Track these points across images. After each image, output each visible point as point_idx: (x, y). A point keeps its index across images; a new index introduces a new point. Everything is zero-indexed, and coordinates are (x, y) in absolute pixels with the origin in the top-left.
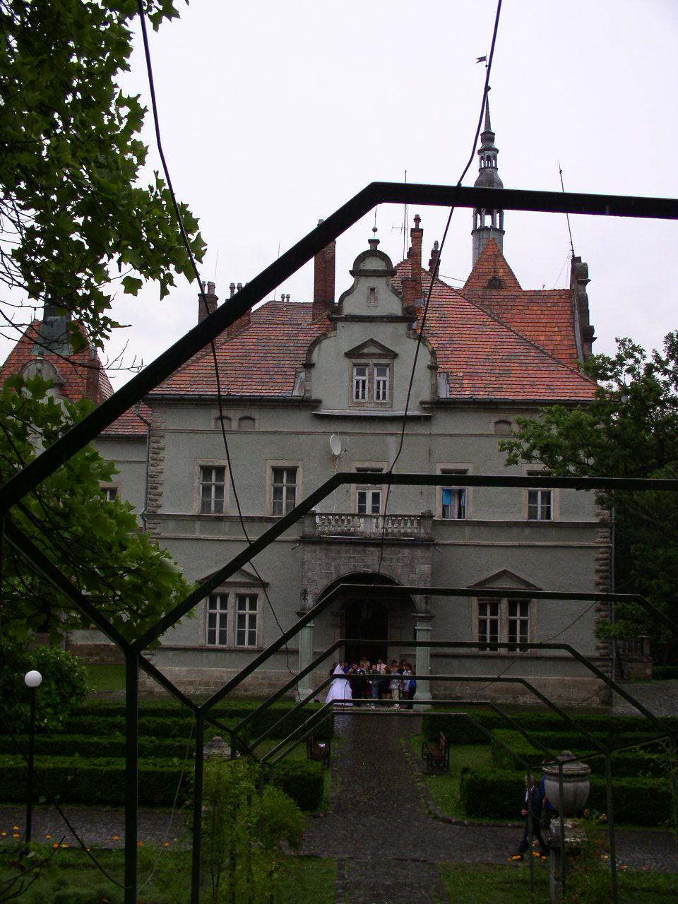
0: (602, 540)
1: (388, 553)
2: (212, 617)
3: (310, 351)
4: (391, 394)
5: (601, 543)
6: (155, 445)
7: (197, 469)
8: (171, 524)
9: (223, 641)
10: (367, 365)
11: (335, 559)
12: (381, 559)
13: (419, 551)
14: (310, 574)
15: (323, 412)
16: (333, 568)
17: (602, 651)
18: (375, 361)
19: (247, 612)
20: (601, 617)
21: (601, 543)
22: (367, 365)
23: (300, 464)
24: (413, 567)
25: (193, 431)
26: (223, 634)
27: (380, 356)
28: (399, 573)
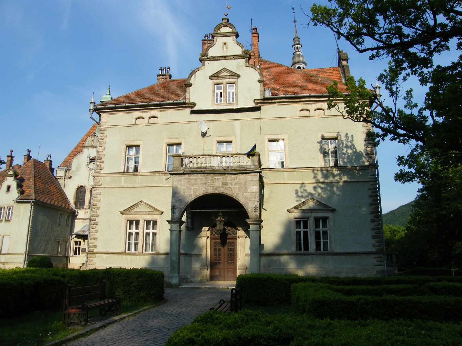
0: (371, 177)
1: (229, 178)
4: (237, 98)
5: (371, 178)
8: (108, 179)
9: (136, 249)
11: (194, 185)
12: (225, 184)
13: (250, 177)
15: (196, 108)
16: (192, 191)
17: (377, 248)
20: (375, 226)
21: (371, 178)
24: (246, 188)
25: (123, 126)
26: (136, 244)
27: (230, 77)
28: (237, 192)
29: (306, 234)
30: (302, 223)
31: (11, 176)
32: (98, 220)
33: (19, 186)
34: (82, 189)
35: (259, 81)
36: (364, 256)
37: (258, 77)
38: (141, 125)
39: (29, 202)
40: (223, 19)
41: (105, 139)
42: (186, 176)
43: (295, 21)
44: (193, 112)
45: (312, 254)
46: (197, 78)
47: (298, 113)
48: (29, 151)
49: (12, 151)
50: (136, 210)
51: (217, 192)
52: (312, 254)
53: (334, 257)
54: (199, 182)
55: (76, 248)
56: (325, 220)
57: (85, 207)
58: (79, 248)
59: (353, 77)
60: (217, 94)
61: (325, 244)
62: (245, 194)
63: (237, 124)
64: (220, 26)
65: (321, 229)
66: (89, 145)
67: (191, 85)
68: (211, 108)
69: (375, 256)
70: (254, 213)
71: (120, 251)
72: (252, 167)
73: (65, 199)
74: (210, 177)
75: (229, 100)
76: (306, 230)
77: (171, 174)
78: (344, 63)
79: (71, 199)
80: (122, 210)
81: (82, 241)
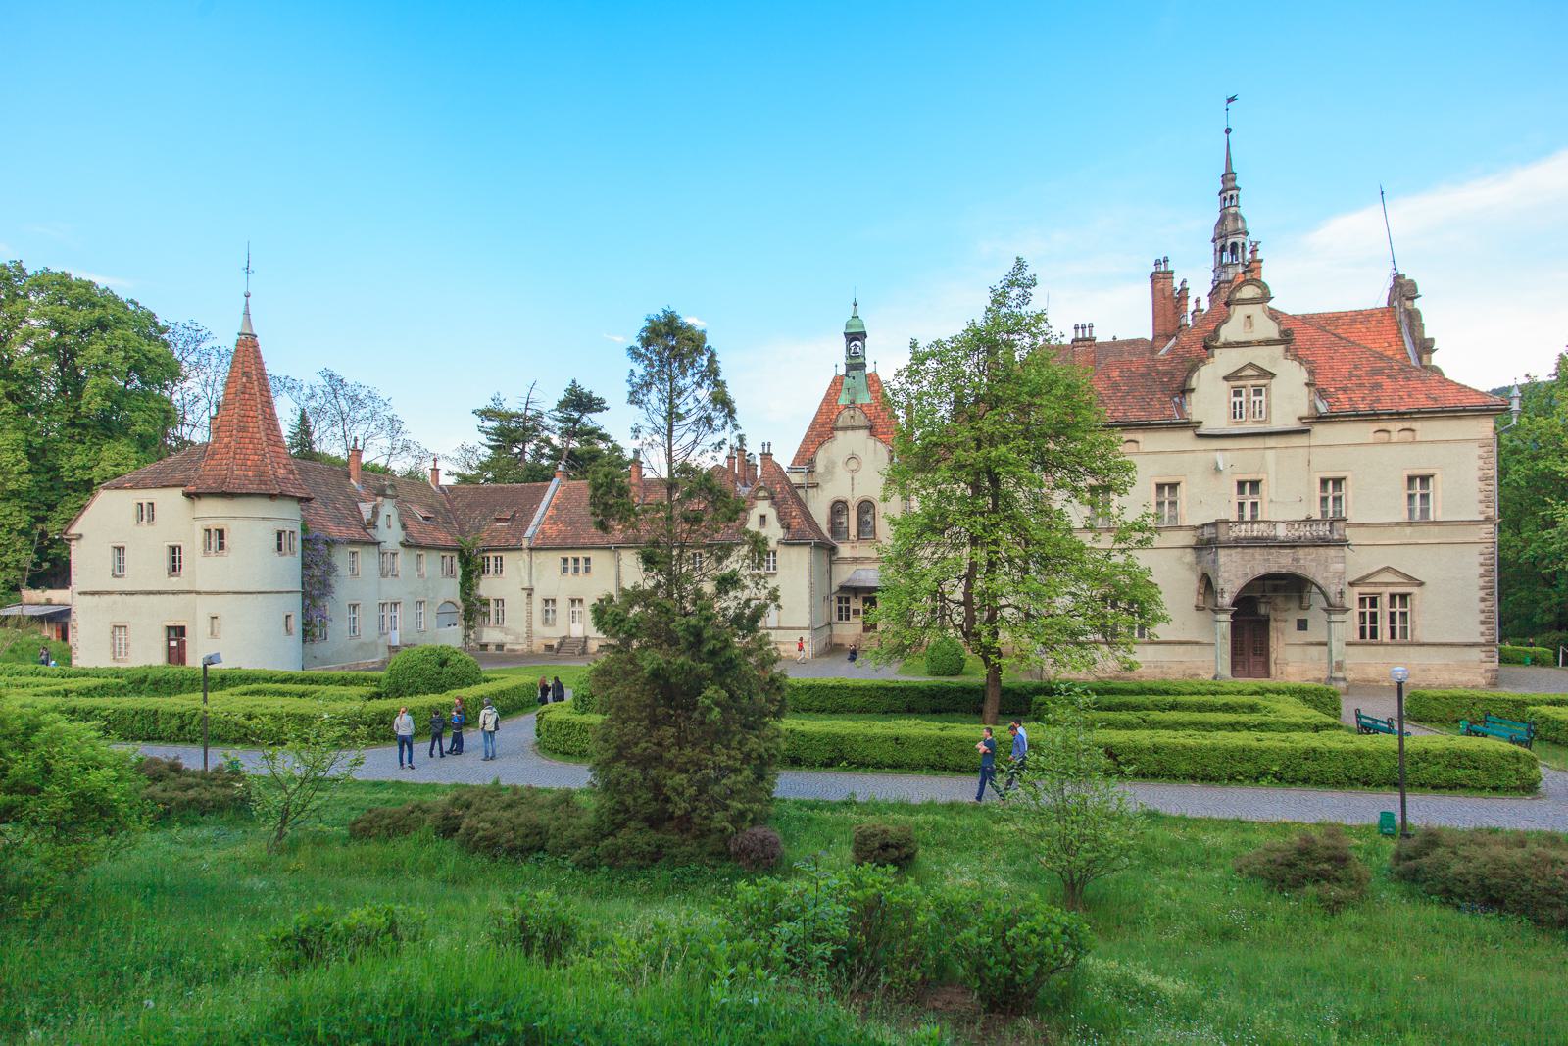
3: (1188, 377)
15: (1202, 431)
18: (1253, 383)
27: (1258, 377)
31: (765, 498)
35: (1307, 385)
37: (1304, 377)
44: (1200, 436)
47: (1371, 438)
55: (840, 609)
57: (851, 538)
60: (1235, 403)
63: (1270, 454)
66: (845, 425)
67: (1192, 390)
79: (824, 527)
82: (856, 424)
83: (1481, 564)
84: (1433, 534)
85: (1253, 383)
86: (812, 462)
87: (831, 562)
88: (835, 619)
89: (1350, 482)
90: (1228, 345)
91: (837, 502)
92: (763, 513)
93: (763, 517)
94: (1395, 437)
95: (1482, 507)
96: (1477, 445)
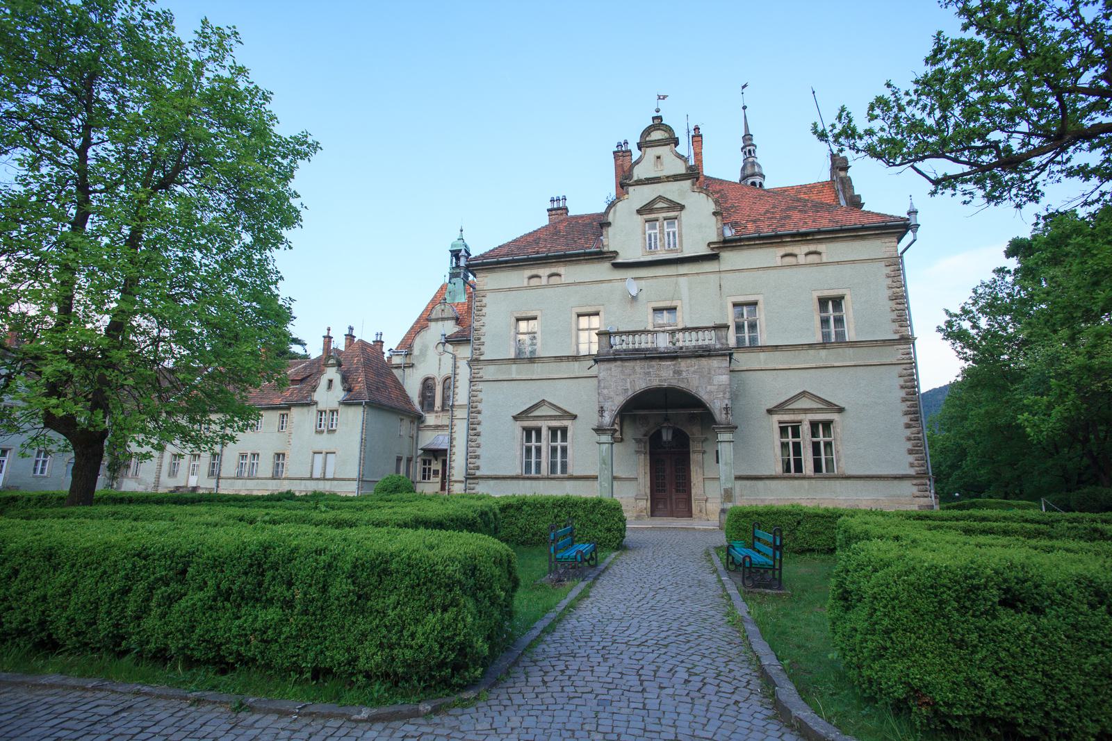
1: (683, 364)
2: (529, 450)
4: (681, 241)
6: (478, 304)
7: (513, 320)
10: (657, 220)
14: (605, 391)
15: (619, 260)
18: (665, 215)
19: (559, 444)
22: (657, 220)
23: (601, 308)
24: (710, 378)
25: (510, 289)
26: (538, 465)
27: (669, 209)
29: (797, 447)
30: (790, 429)
31: (333, 365)
32: (479, 429)
33: (345, 379)
34: (430, 382)
35: (714, 214)
36: (896, 482)
37: (712, 207)
38: (538, 287)
39: (360, 404)
40: (654, 118)
41: (485, 310)
42: (619, 363)
43: (744, 108)
45: (810, 478)
46: (617, 214)
47: (779, 262)
48: (351, 329)
49: (329, 329)
50: (536, 413)
51: (665, 385)
52: (810, 478)
53: (844, 482)
54: (638, 369)
55: (425, 470)
56: (827, 425)
57: (436, 409)
58: (430, 469)
59: (859, 196)
60: (650, 236)
61: (829, 462)
62: (709, 387)
63: (682, 280)
64: (648, 131)
65: (821, 439)
67: (609, 224)
68: (642, 259)
69: (915, 482)
70: (724, 416)
71: (513, 473)
72: (718, 346)
73: (407, 399)
74: (654, 363)
75: (669, 244)
76: (796, 440)
77: (596, 361)
78: (842, 174)
79: (416, 400)
80: (515, 414)
81: (432, 458)
82: (445, 315)
83: (902, 387)
84: (848, 356)
85: (665, 215)
86: (410, 347)
87: (419, 429)
88: (419, 478)
89: (761, 306)
90: (640, 182)
91: (427, 379)
92: (330, 378)
93: (331, 381)
94: (802, 259)
95: (895, 326)
96: (883, 264)
